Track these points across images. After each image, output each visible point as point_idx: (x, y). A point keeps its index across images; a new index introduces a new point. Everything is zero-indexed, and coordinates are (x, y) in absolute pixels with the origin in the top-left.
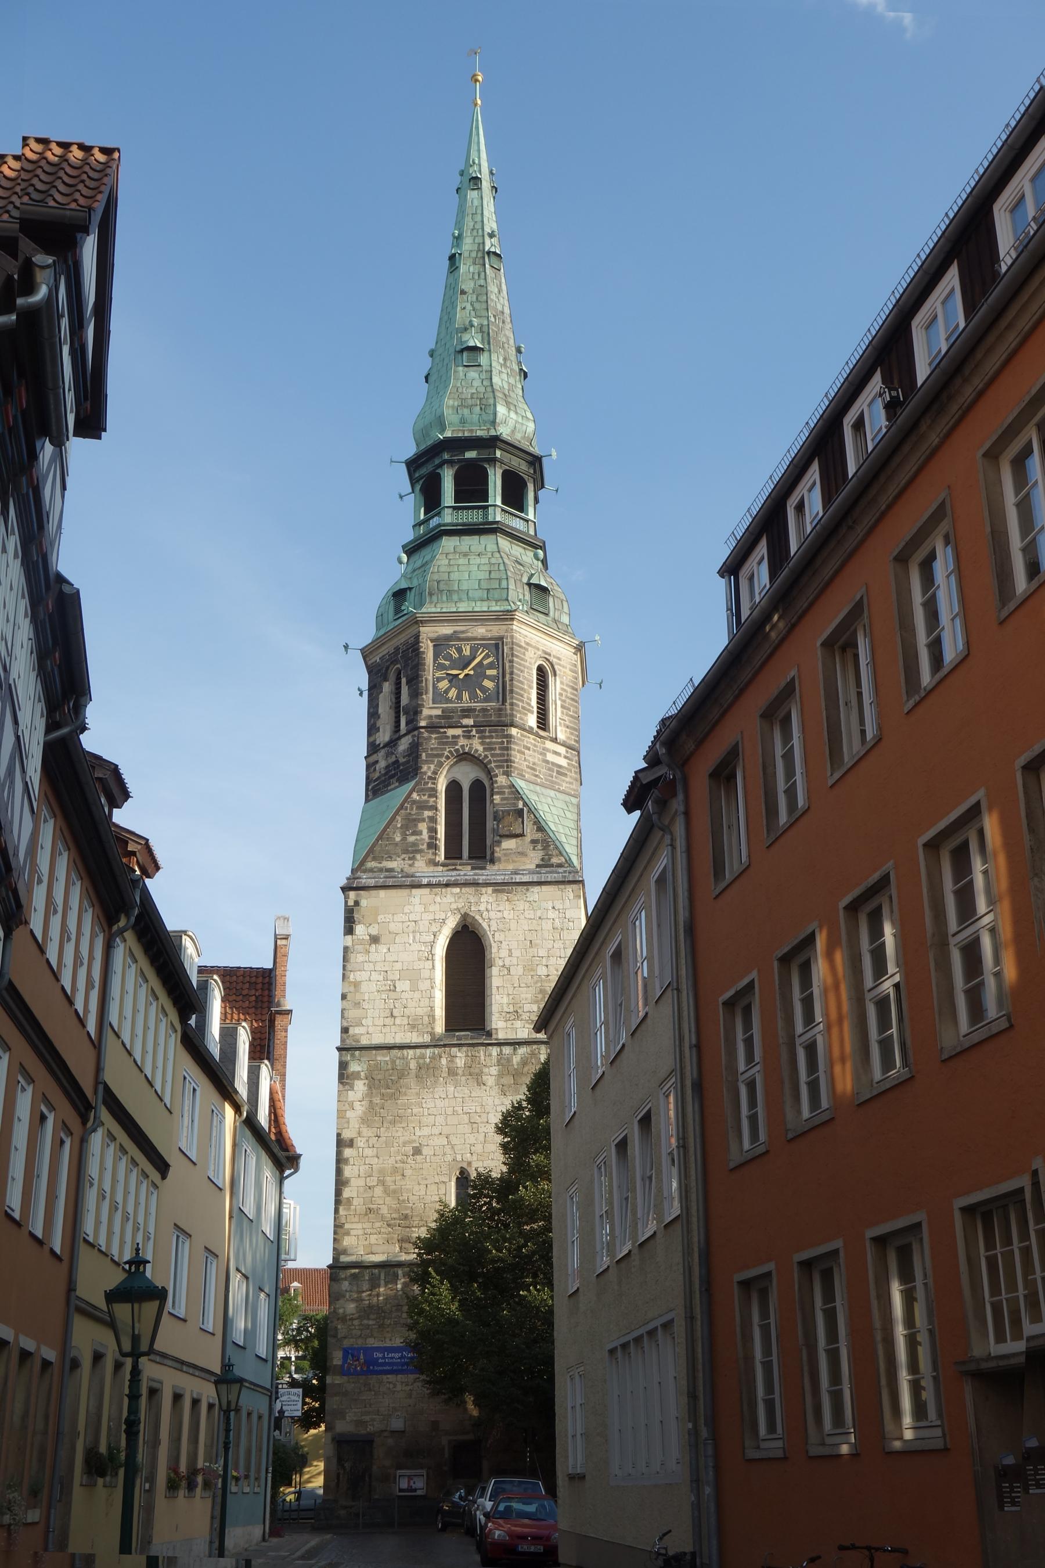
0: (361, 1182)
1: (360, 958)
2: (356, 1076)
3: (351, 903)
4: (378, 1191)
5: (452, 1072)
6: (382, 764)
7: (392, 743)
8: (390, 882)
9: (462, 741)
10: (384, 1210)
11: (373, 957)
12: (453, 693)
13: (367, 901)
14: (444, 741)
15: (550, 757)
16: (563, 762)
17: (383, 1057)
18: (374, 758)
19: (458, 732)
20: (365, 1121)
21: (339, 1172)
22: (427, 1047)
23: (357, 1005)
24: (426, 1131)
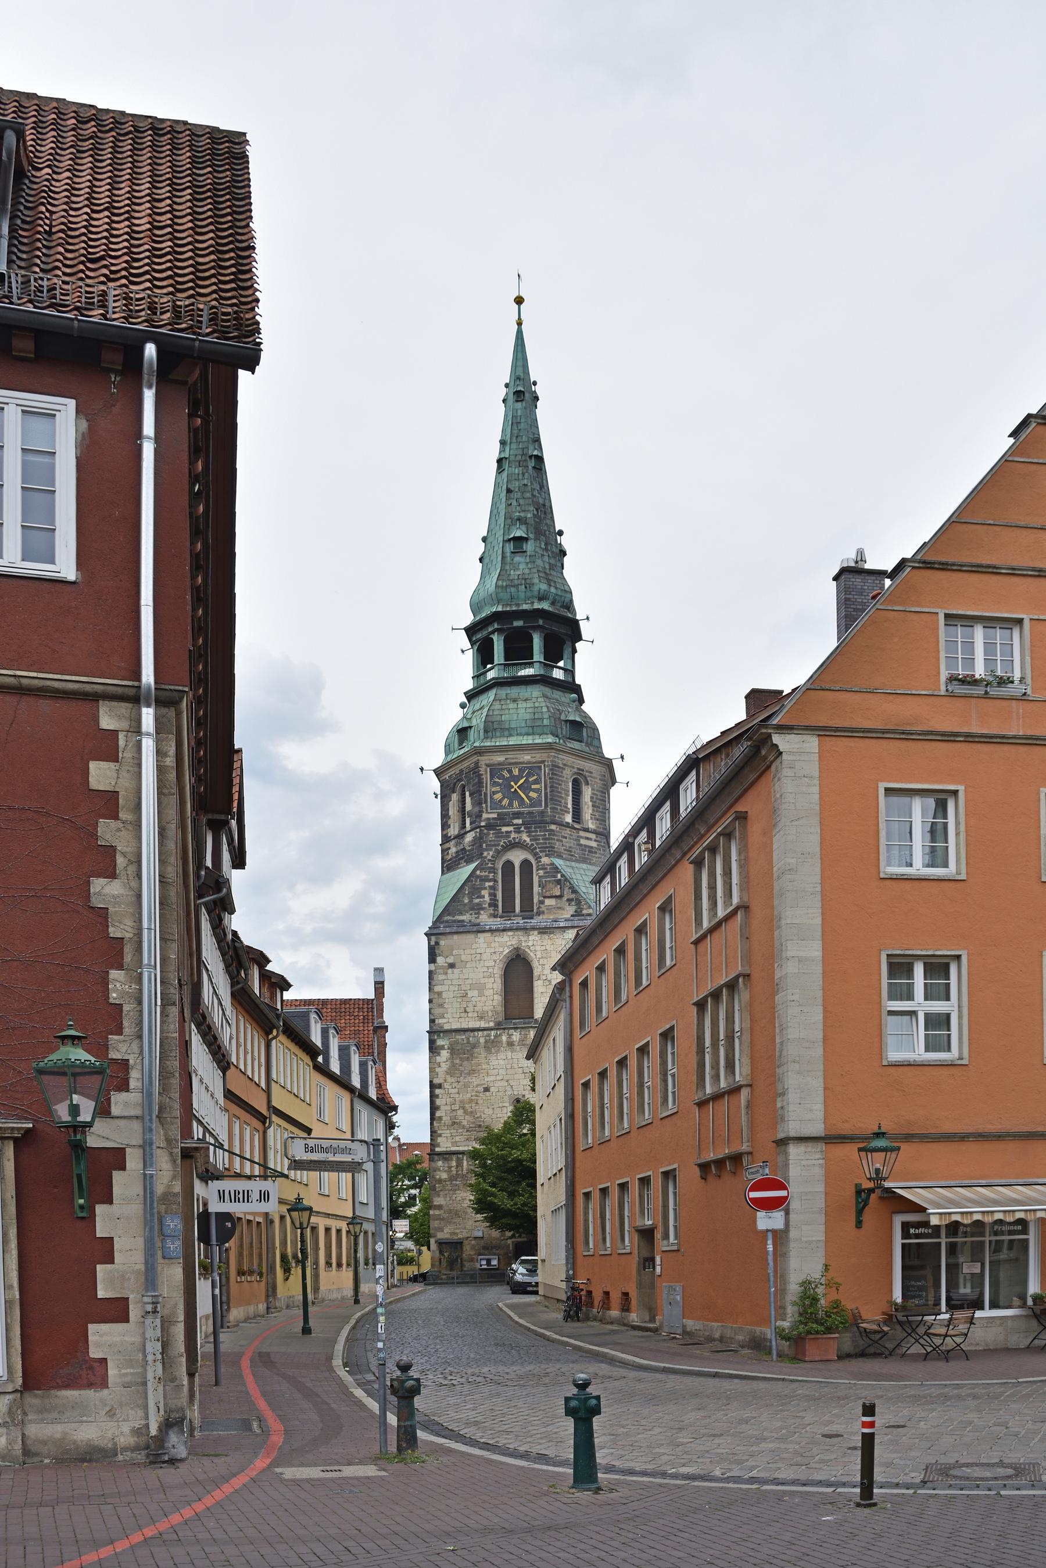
1: (441, 977)
2: (442, 1047)
4: (460, 1112)
5: (510, 1044)
6: (453, 850)
7: (460, 836)
8: (461, 929)
9: (513, 835)
10: (465, 1123)
11: (450, 976)
12: (505, 802)
14: (499, 835)
15: (583, 842)
16: (594, 844)
18: (447, 845)
20: (449, 1072)
22: (491, 1029)
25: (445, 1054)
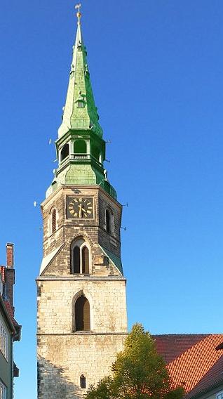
0: (47, 378)
1: (44, 304)
3: (39, 285)
9: (79, 232)
11: (48, 304)
13: (45, 285)
14: (73, 231)
17: (53, 337)
19: (78, 228)
21: (38, 375)
23: (44, 320)
24: (69, 362)
25: (45, 347)
